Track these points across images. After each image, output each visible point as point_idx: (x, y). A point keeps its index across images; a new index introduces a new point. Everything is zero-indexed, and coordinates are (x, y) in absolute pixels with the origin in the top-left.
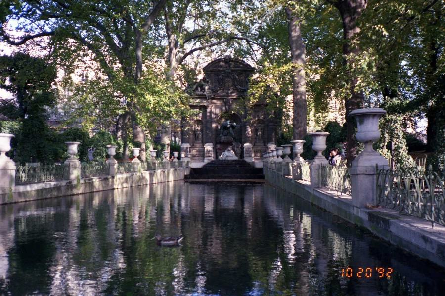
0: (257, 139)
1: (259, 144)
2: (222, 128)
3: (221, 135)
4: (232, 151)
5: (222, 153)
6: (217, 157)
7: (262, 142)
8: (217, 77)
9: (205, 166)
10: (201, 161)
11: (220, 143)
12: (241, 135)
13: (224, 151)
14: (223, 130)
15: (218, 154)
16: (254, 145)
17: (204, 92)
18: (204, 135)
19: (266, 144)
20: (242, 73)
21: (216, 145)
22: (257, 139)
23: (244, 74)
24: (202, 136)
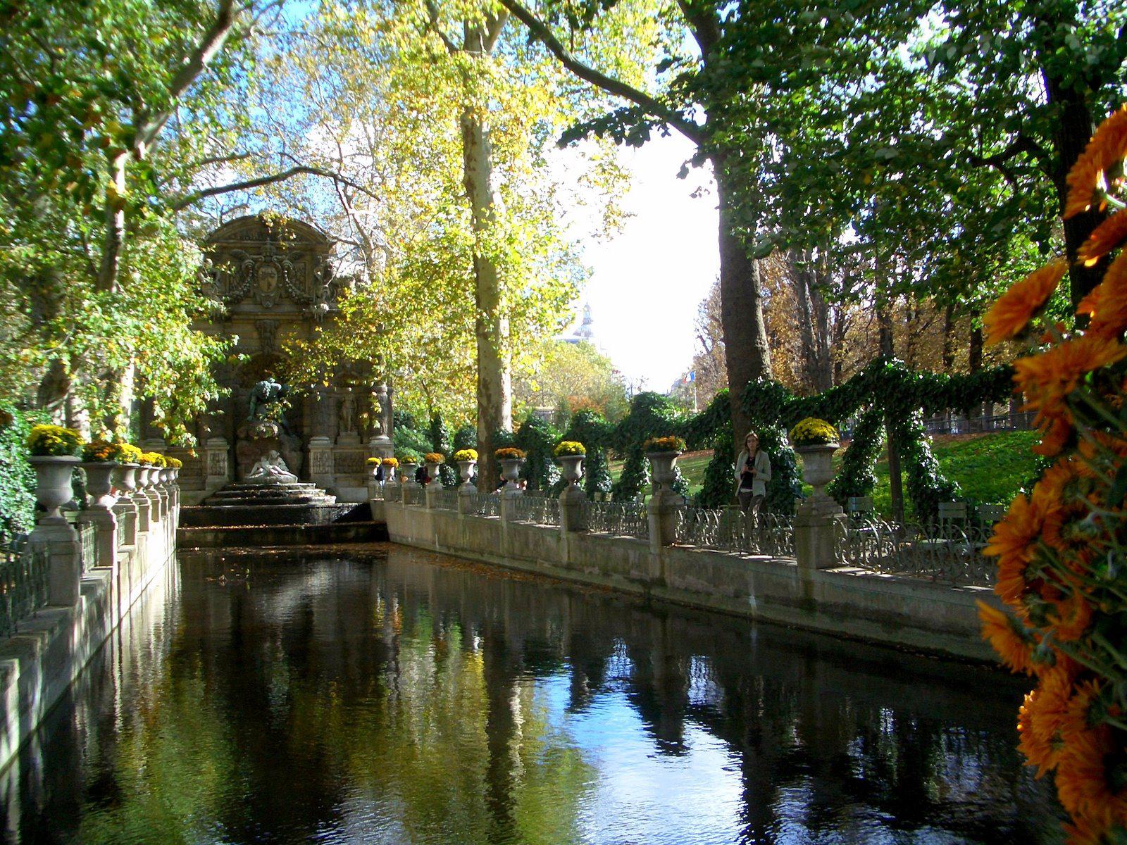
0: (342, 428)
1: (347, 440)
2: (253, 399)
3: (250, 418)
4: (280, 460)
5: (252, 466)
6: (236, 475)
7: (355, 433)
10: (193, 487)
12: (302, 416)
14: (256, 404)
15: (242, 468)
16: (336, 442)
19: (365, 440)
22: (342, 428)
23: (308, 258)
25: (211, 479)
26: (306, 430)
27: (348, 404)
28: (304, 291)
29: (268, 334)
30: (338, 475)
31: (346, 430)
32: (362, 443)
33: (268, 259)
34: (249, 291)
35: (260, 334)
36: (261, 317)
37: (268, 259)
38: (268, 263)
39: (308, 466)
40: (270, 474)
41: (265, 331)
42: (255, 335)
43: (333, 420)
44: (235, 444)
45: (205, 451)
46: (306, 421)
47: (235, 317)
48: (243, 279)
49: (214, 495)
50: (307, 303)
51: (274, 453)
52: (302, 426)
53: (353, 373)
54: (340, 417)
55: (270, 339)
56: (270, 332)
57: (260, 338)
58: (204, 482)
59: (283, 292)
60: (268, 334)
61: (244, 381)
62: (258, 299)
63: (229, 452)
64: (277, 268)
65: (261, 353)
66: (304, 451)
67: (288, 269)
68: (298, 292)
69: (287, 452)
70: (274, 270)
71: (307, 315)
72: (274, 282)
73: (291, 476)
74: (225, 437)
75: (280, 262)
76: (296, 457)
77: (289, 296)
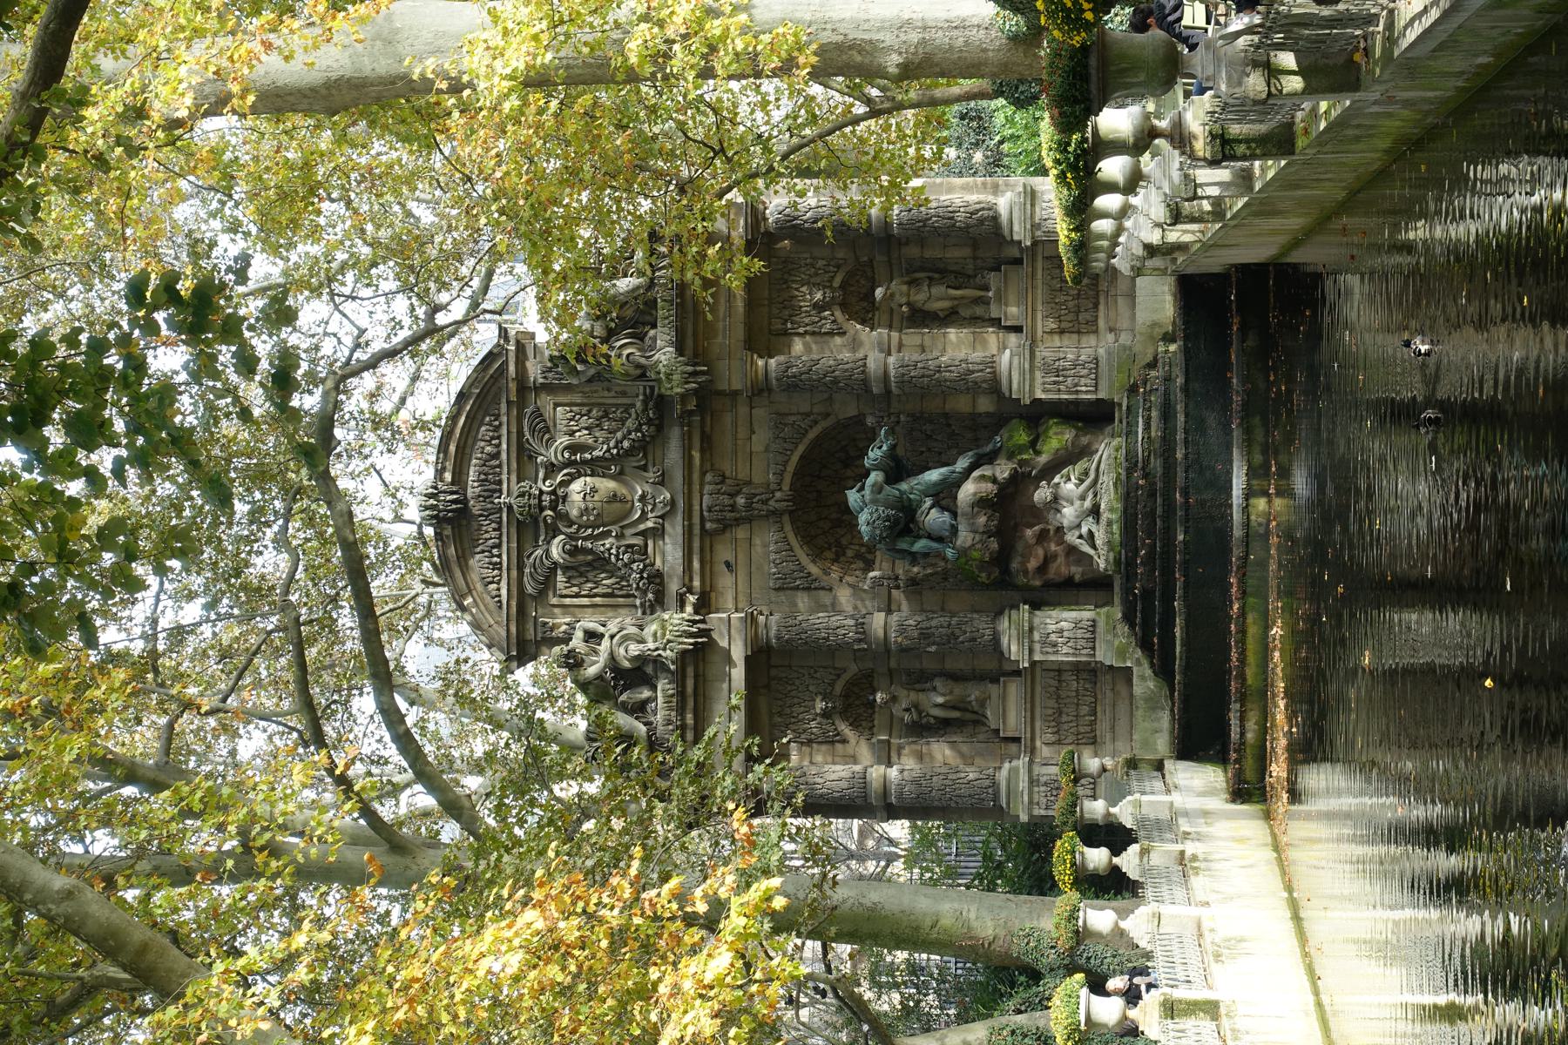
0: (979, 311)
3: (950, 553)
4: (1056, 480)
5: (1072, 550)
7: (993, 279)
8: (561, 577)
9: (1164, 671)
11: (1002, 559)
12: (946, 415)
13: (1060, 530)
15: (1077, 572)
16: (1017, 329)
17: (658, 663)
18: (950, 665)
19: (1015, 253)
20: (538, 413)
21: (1016, 588)
22: (979, 311)
24: (956, 677)
25: (1104, 655)
26: (985, 405)
27: (920, 297)
28: (627, 408)
29: (741, 501)
30: (1101, 323)
31: (985, 302)
32: (1018, 262)
33: (546, 498)
34: (628, 546)
35: (738, 522)
36: (696, 520)
37: (546, 498)
38: (559, 499)
39: (1077, 403)
40: (1095, 512)
41: (733, 507)
42: (741, 533)
43: (953, 333)
44: (1016, 588)
45: (1033, 664)
46: (962, 404)
47: (696, 583)
48: (600, 563)
49: (1145, 645)
50: (659, 405)
51: (1042, 494)
52: (974, 415)
53: (837, 283)
54: (949, 318)
55: (750, 497)
56: (732, 495)
57: (749, 520)
58: (1111, 667)
59: (634, 462)
60: (741, 501)
61: (859, 556)
62: (650, 524)
63: (1036, 606)
64: (572, 478)
65: (786, 518)
66: (1037, 415)
67: (574, 449)
68: (629, 423)
69: (1043, 459)
70: (576, 486)
71: (691, 406)
72: (607, 485)
73: (1107, 451)
74: (999, 613)
75: (551, 469)
76: (1058, 438)
77: (642, 447)
